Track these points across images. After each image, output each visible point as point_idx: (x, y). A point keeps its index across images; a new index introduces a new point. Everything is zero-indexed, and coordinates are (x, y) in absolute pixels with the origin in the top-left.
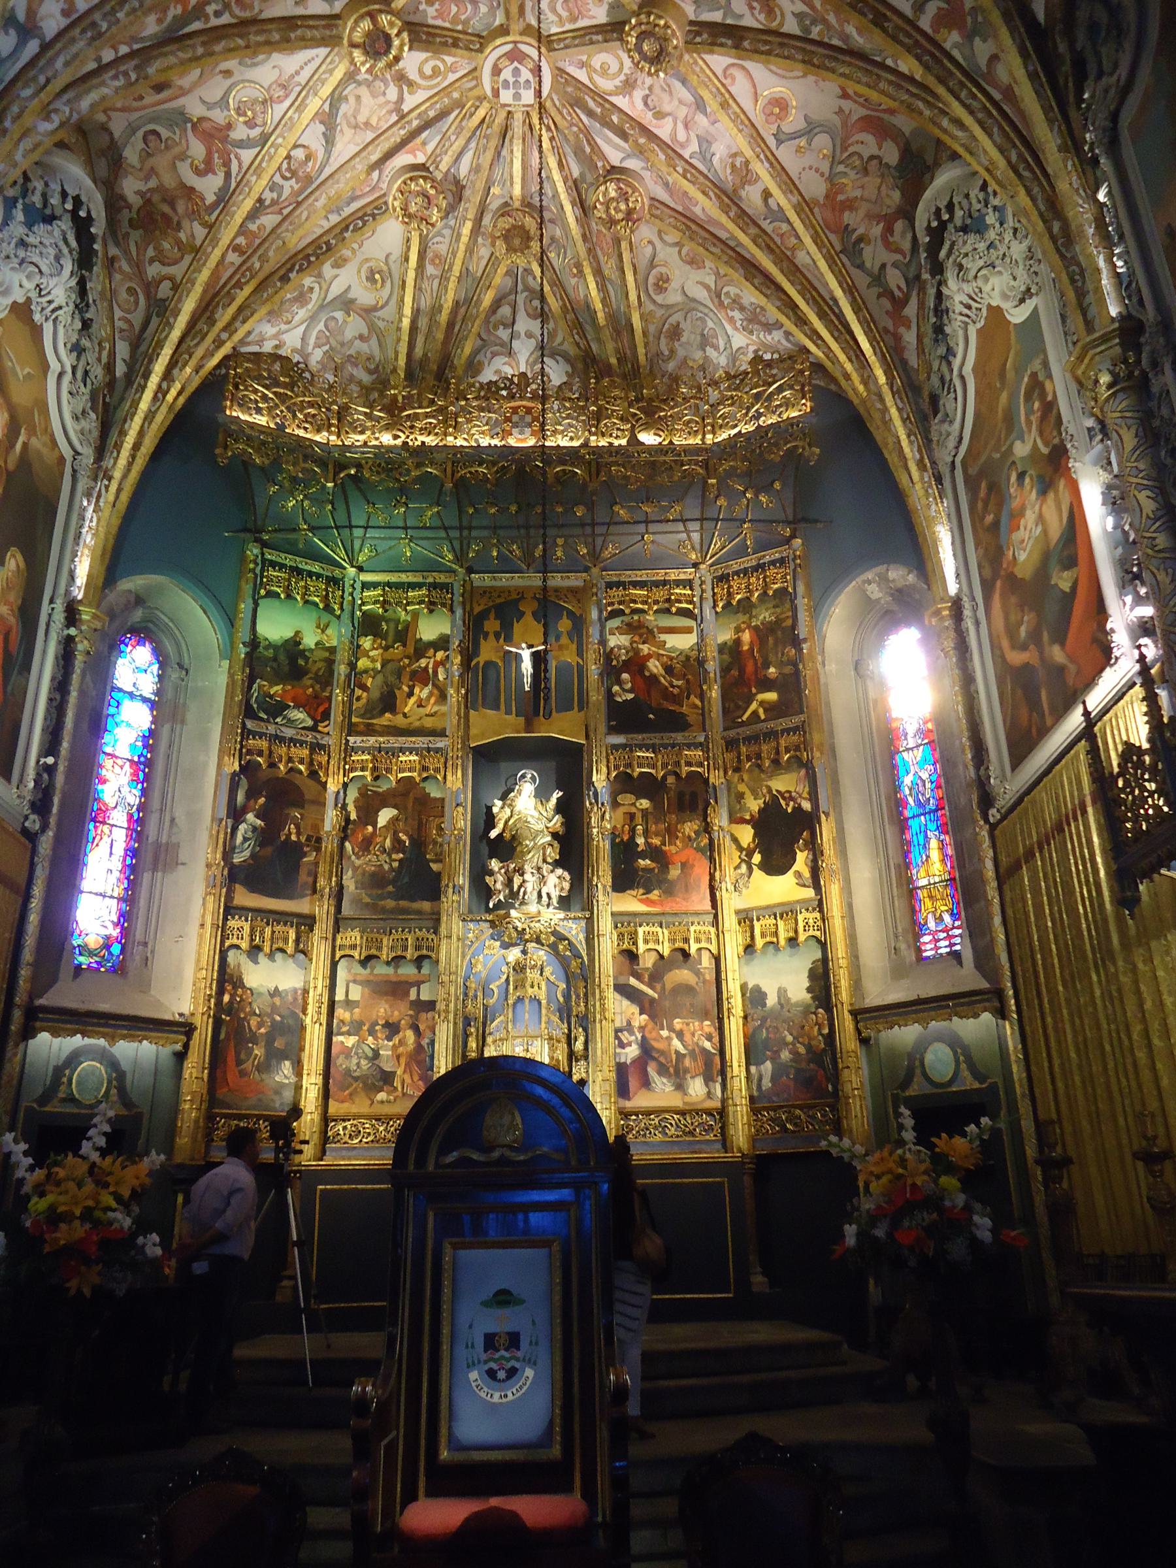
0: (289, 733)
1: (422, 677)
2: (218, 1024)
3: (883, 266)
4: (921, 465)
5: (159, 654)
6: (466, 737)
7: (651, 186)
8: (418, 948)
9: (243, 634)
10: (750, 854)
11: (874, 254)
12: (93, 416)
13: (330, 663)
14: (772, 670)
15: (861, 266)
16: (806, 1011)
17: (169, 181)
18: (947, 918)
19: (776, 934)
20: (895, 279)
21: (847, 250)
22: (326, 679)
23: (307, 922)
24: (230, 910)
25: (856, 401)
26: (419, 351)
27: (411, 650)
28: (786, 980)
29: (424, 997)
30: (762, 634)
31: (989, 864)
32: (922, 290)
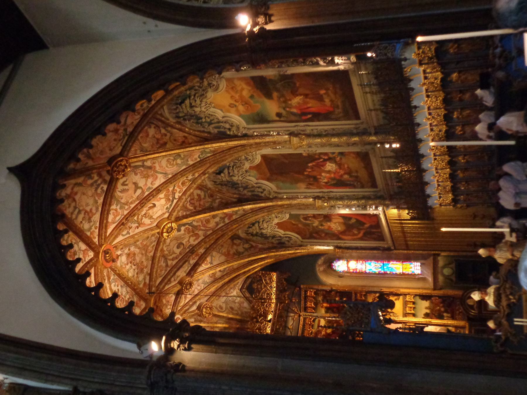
3: (244, 248)
4: (296, 250)
7: (204, 300)
10: (388, 312)
11: (241, 249)
14: (337, 299)
15: (243, 253)
16: (432, 302)
18: (411, 266)
19: (411, 307)
20: (246, 246)
21: (239, 255)
25: (274, 262)
28: (424, 306)
30: (325, 300)
31: (403, 252)
32: (250, 240)
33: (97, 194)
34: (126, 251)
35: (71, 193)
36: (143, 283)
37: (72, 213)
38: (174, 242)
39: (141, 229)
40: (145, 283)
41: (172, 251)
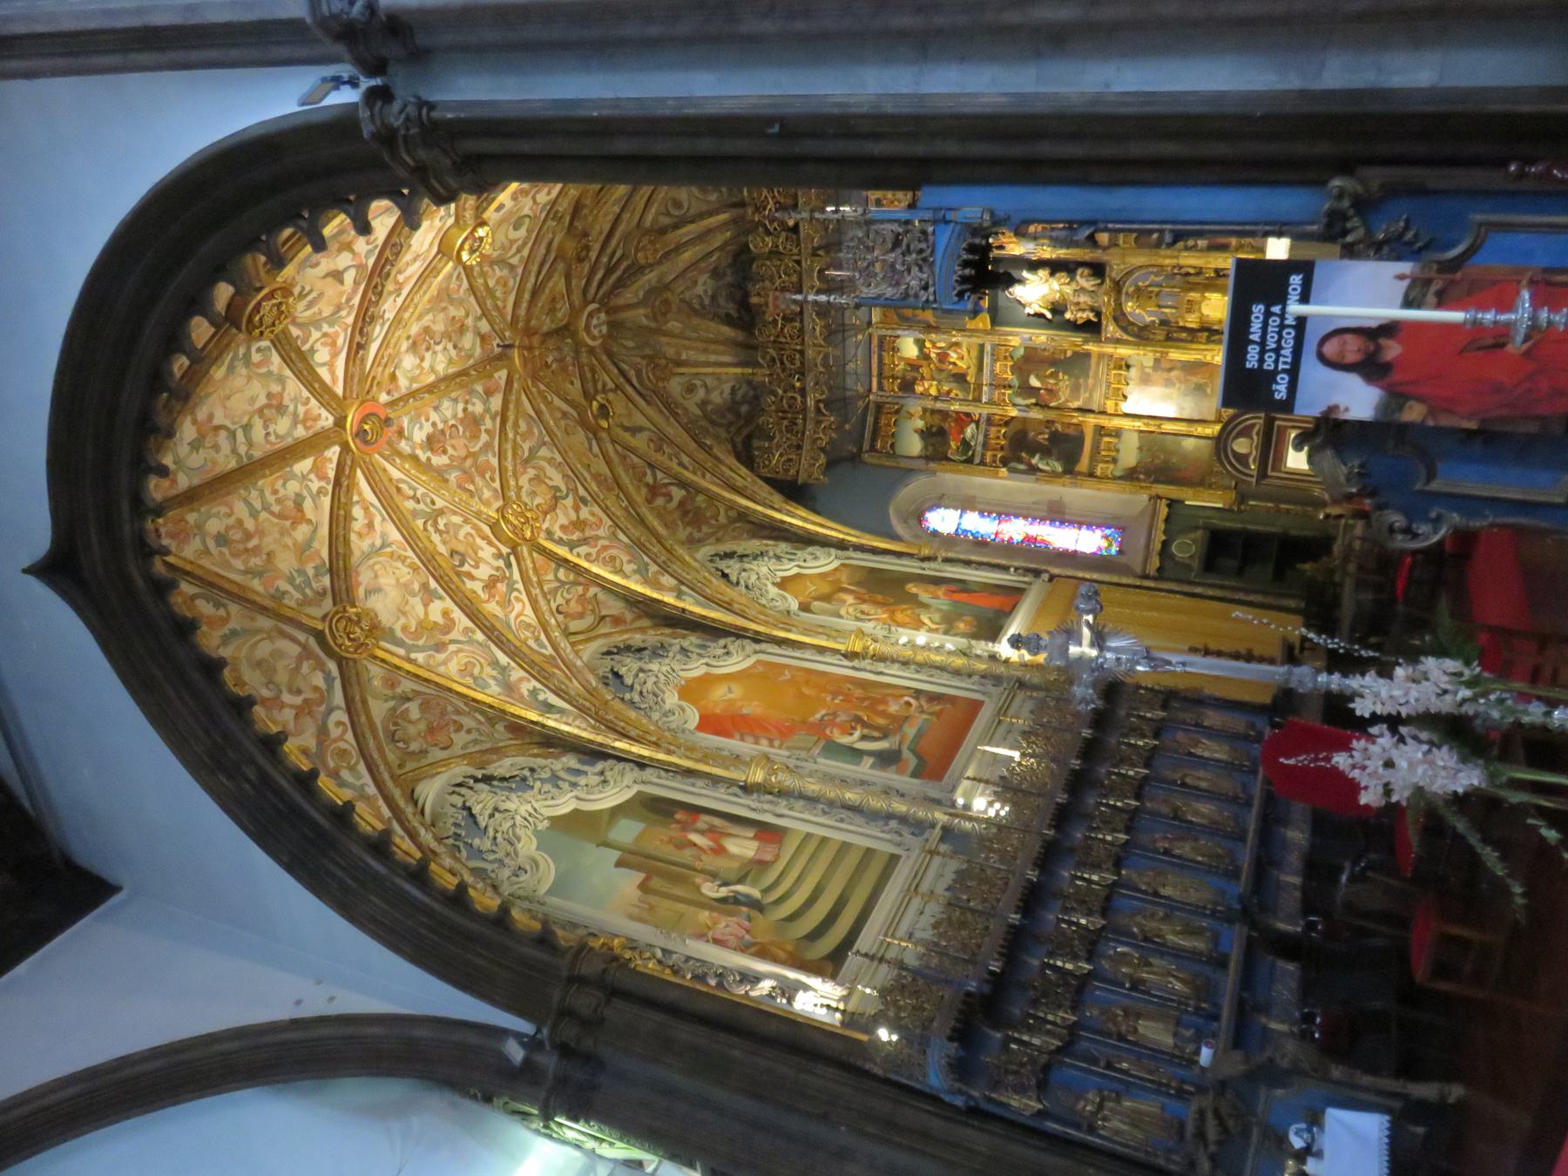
0: (981, 438)
1: (943, 357)
2: (1157, 481)
5: (931, 509)
6: (986, 332)
8: (1120, 368)
9: (921, 464)
12: (810, 549)
13: (933, 412)
17: (677, 515)
22: (945, 414)
23: (1100, 431)
24: (1091, 475)
26: (726, 359)
27: (924, 363)
29: (1151, 363)
33: (259, 365)
34: (405, 345)
35: (199, 432)
36: (478, 340)
37: (234, 451)
38: (502, 229)
39: (405, 292)
40: (483, 338)
41: (507, 244)
